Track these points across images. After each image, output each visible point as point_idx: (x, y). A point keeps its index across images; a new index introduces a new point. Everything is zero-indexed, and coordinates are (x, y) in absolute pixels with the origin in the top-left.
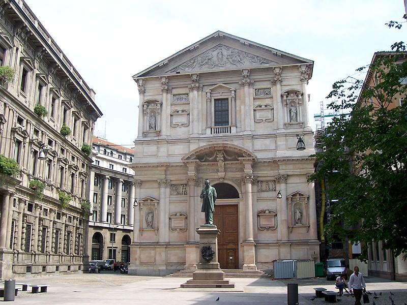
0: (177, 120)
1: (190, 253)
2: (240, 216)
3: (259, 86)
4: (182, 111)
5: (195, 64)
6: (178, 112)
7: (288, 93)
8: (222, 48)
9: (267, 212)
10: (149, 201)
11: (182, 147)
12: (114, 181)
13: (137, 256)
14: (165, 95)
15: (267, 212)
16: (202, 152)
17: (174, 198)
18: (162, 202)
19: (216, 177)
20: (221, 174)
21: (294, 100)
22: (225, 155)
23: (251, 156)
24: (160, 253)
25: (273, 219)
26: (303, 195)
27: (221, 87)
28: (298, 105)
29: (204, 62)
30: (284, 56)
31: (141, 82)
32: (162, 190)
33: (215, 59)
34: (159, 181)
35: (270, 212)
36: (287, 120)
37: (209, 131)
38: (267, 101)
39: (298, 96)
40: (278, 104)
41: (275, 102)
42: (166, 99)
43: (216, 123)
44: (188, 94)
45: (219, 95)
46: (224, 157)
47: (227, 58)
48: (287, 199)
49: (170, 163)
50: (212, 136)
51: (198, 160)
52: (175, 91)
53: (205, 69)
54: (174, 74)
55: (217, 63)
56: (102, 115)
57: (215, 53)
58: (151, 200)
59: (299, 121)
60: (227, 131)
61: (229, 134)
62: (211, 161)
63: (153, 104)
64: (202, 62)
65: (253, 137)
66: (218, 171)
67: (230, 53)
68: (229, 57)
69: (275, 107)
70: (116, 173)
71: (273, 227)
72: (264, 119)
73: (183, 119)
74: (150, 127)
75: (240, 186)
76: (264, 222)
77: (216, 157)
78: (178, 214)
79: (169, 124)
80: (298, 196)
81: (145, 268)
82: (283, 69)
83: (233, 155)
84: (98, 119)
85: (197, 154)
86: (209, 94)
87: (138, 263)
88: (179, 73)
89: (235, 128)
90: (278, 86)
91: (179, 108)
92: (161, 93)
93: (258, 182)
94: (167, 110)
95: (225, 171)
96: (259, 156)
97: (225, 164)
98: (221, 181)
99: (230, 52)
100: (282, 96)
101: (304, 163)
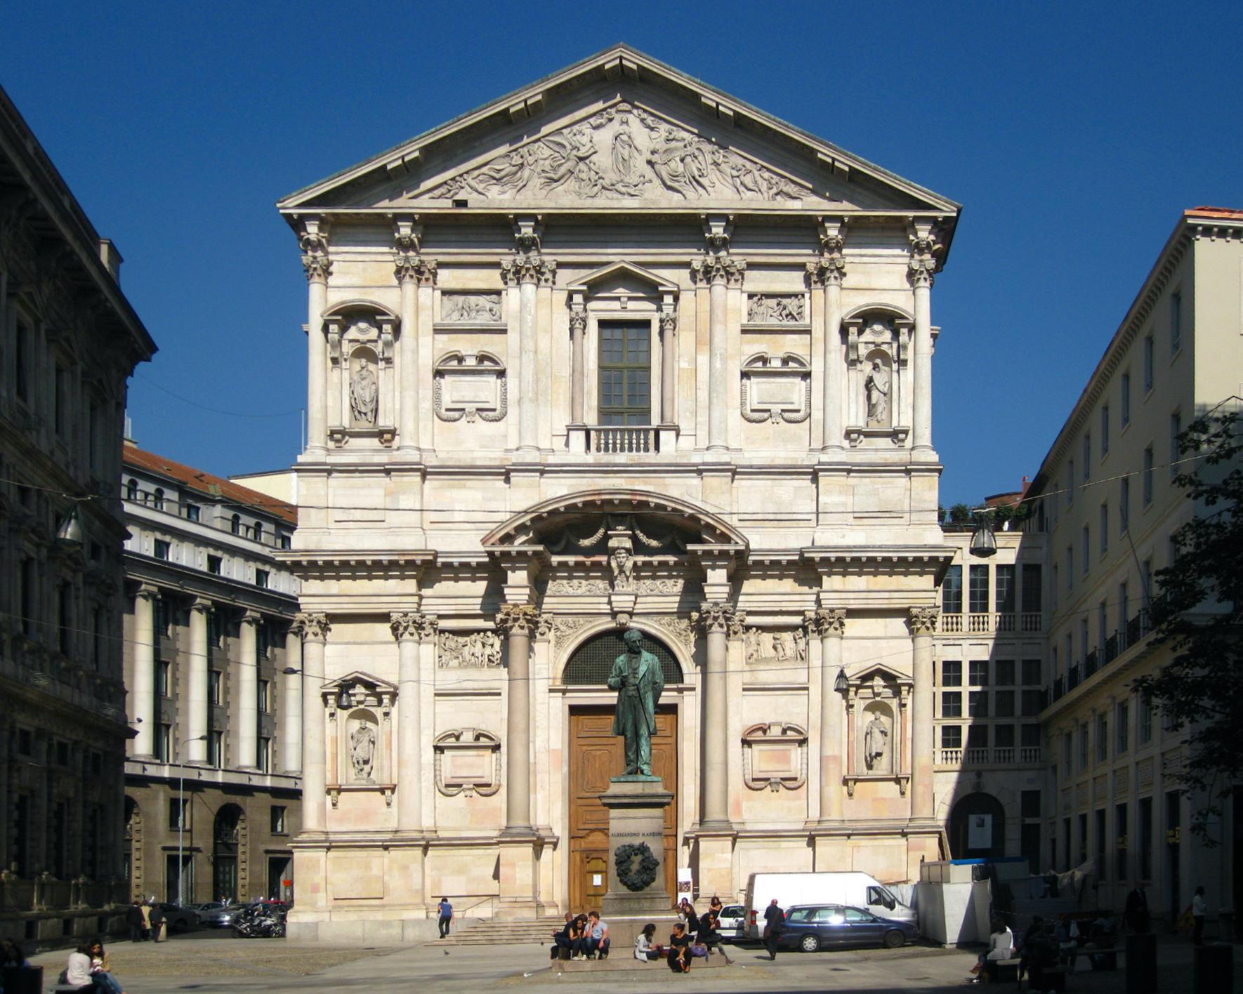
0: (455, 389)
1: (513, 865)
3: (759, 281)
4: (482, 358)
5: (526, 172)
6: (460, 360)
7: (869, 317)
8: (631, 118)
11: (479, 495)
12: (223, 623)
13: (319, 879)
14: (409, 286)
16: (558, 519)
17: (452, 678)
18: (406, 693)
21: (884, 347)
23: (727, 539)
24: (405, 868)
26: (894, 678)
27: (623, 277)
28: (895, 366)
29: (563, 170)
31: (312, 230)
32: (409, 646)
33: (603, 160)
34: (394, 617)
36: (857, 418)
37: (578, 438)
38: (794, 345)
39: (896, 334)
40: (826, 355)
41: (818, 348)
42: (417, 306)
43: (605, 413)
44: (498, 293)
45: (616, 305)
46: (634, 538)
47: (650, 162)
49: (436, 554)
50: (591, 458)
51: (540, 548)
53: (566, 199)
54: (444, 205)
55: (610, 177)
56: (153, 348)
57: (604, 137)
58: (370, 686)
59: (895, 424)
60: (646, 443)
61: (650, 457)
62: (588, 552)
63: (362, 325)
64: (554, 169)
65: (735, 472)
68: (655, 158)
69: (816, 368)
70: (232, 588)
71: (795, 779)
72: (776, 409)
73: (485, 389)
77: (607, 537)
78: (467, 738)
79: (427, 405)
81: (352, 917)
83: (676, 538)
84: (141, 367)
85: (539, 525)
86: (578, 298)
87: (322, 900)
88: (463, 204)
89: (673, 434)
90: (833, 290)
91: (468, 347)
93: (748, 628)
94: (419, 349)
96: (760, 541)
98: (623, 619)
99: (665, 135)
100: (844, 330)
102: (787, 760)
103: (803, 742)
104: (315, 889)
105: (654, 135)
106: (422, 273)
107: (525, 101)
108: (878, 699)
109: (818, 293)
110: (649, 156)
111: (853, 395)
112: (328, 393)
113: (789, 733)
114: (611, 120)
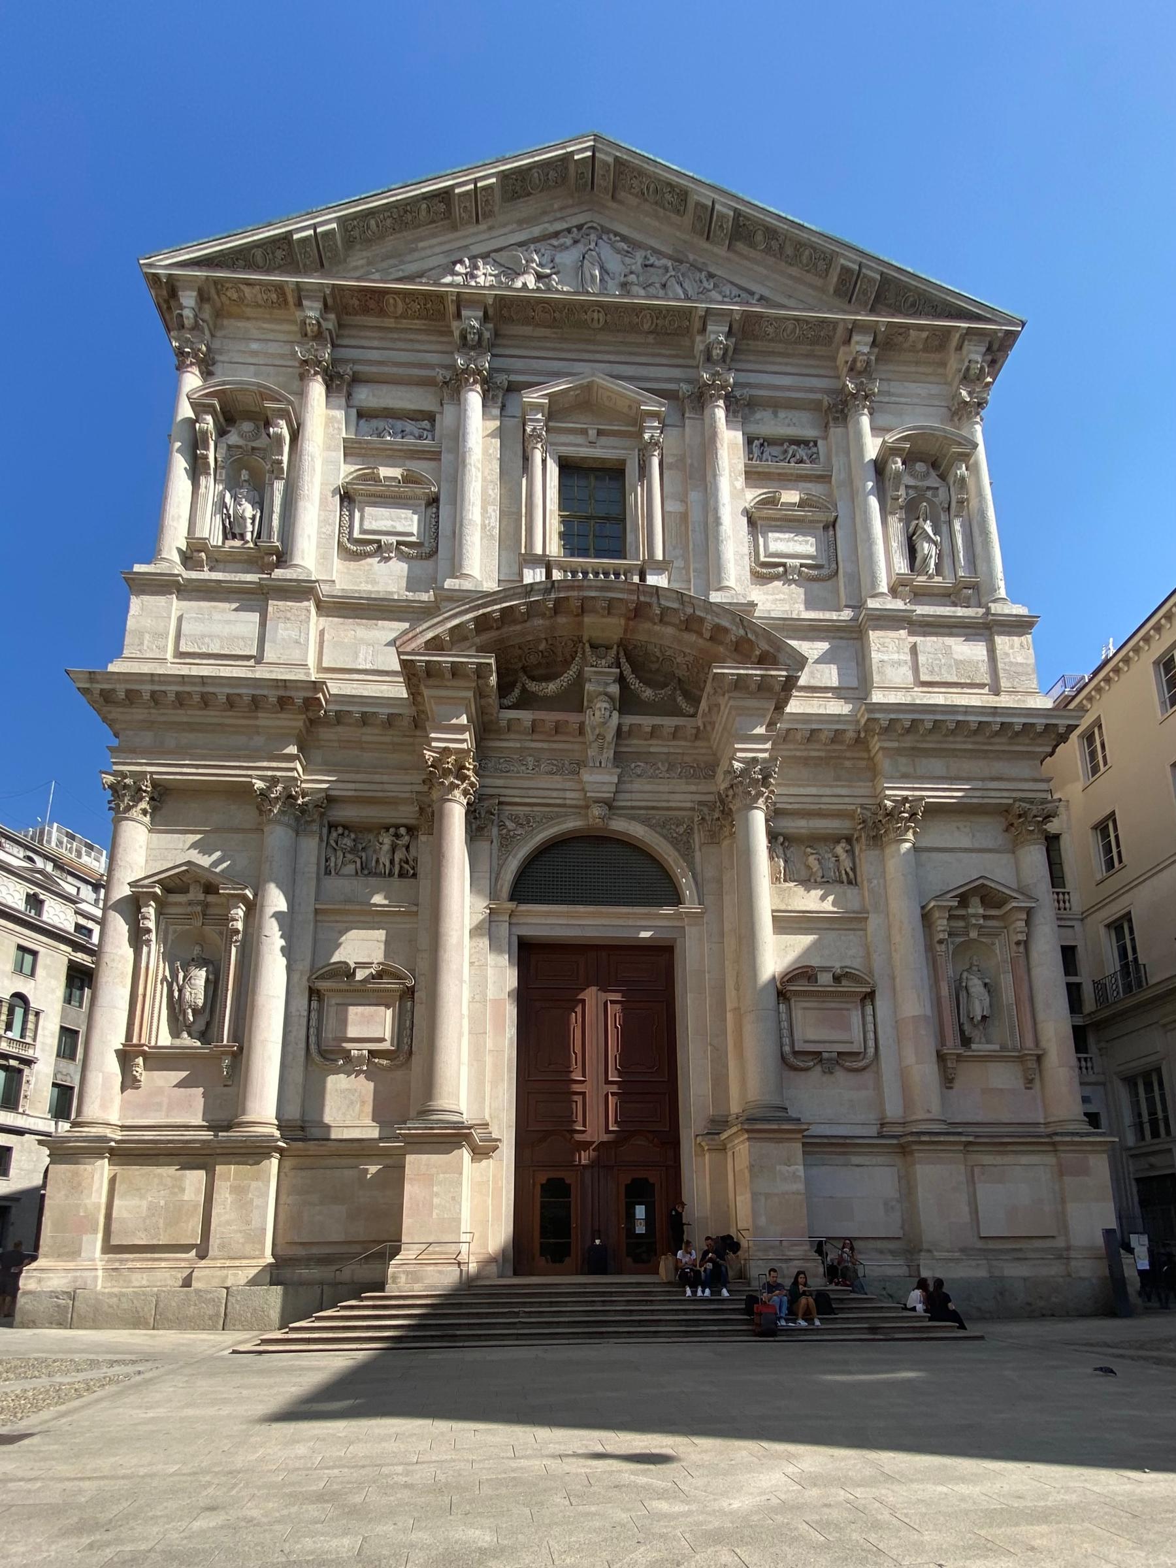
2: (690, 997)
9: (825, 979)
10: (196, 894)
15: (825, 979)
19: (572, 797)
20: (600, 779)
22: (631, 678)
25: (855, 1017)
30: (895, 291)
35: (837, 979)
36: (901, 565)
48: (926, 917)
52: (365, 396)
66: (581, 764)
67: (637, 267)
74: (231, 530)
75: (685, 848)
76: (811, 1028)
80: (976, 908)
82: (887, 344)
92: (296, 384)
95: (619, 759)
97: (619, 727)
99: (640, 261)
101: (1000, 755)
102: (847, 1027)
103: (870, 996)
104: (84, 1225)
105: (628, 260)
106: (331, 379)
107: (475, 181)
108: (973, 934)
109: (835, 432)
110: (622, 279)
111: (895, 545)
112: (190, 508)
113: (844, 982)
114: (576, 242)
